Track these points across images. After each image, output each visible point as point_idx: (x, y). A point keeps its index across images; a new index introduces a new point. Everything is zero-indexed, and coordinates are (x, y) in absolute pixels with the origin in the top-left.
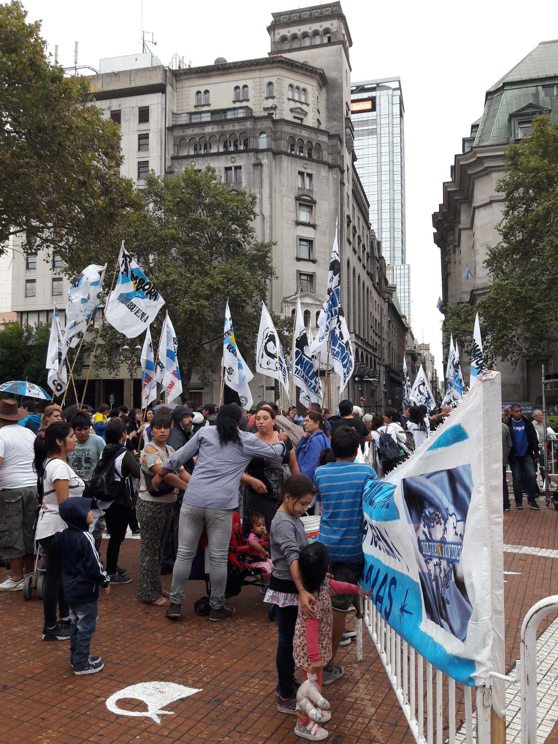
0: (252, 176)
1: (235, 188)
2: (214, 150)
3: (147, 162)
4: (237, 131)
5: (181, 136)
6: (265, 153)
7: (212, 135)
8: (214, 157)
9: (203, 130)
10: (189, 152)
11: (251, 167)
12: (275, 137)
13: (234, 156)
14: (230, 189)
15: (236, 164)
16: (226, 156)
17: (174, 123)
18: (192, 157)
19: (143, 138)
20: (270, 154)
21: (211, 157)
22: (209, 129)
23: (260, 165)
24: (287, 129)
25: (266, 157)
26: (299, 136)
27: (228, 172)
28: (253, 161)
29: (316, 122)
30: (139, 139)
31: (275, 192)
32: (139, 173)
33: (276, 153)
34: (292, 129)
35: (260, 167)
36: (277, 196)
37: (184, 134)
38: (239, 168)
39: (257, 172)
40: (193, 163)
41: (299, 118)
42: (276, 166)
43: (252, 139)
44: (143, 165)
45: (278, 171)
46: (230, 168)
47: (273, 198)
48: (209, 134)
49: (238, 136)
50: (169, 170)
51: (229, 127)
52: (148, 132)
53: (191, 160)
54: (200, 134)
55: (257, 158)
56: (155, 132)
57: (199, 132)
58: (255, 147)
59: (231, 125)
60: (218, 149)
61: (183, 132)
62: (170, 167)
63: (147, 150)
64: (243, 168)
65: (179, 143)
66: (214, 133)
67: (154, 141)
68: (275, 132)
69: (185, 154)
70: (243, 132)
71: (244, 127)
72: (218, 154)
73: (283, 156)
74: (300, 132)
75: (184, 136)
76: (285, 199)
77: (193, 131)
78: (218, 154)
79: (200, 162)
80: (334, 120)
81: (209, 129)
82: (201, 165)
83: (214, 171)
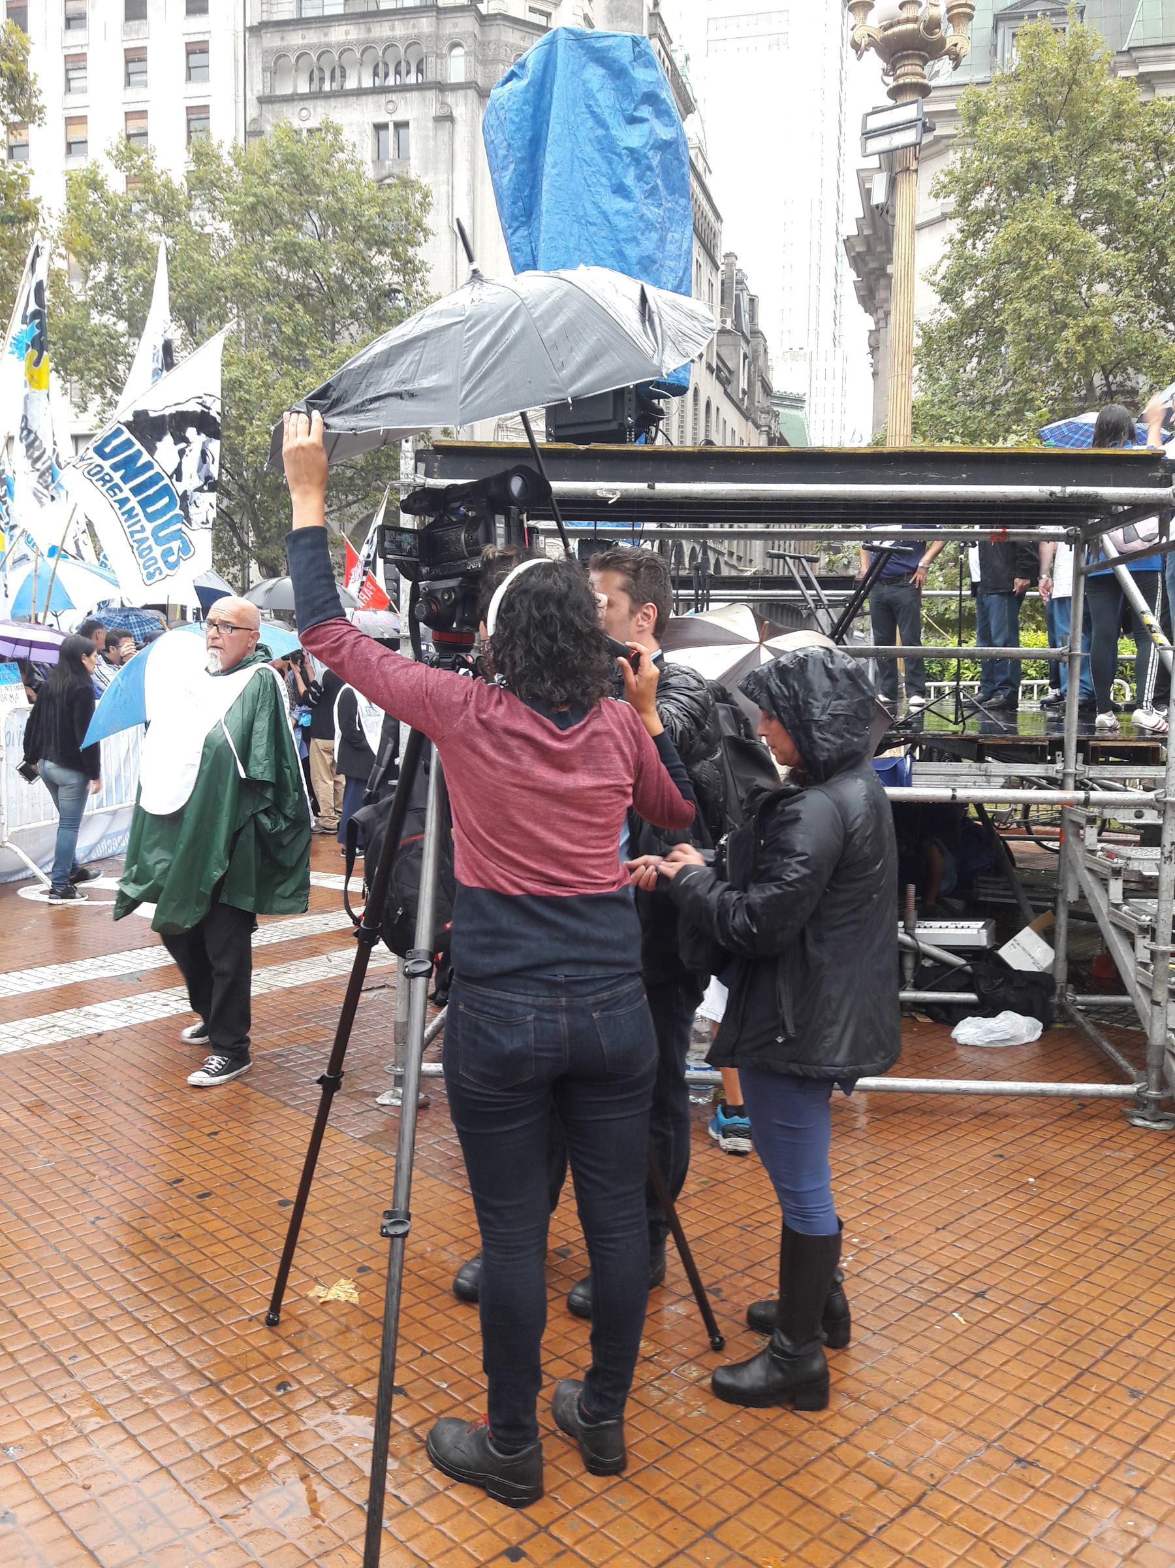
0: (432, 143)
1: (396, 171)
2: (351, 84)
5: (279, 50)
6: (461, 93)
7: (345, 50)
8: (352, 99)
9: (326, 35)
10: (295, 86)
11: (430, 124)
12: (483, 55)
13: (393, 97)
14: (385, 173)
15: (399, 117)
16: (376, 97)
17: (265, 18)
18: (303, 97)
20: (472, 94)
21: (342, 100)
22: (339, 34)
23: (450, 118)
24: (512, 36)
25: (462, 101)
27: (382, 133)
28: (434, 110)
29: (581, 21)
30: (188, 53)
32: (189, 132)
34: (523, 39)
35: (448, 124)
38: (406, 124)
39: (443, 135)
40: (304, 113)
41: (542, 13)
44: (197, 115)
46: (385, 126)
47: (478, 193)
48: (340, 44)
51: (382, 30)
55: (443, 104)
58: (439, 79)
59: (386, 25)
61: (282, 39)
62: (254, 120)
63: (206, 79)
65: (276, 65)
68: (484, 45)
69: (287, 90)
70: (413, 43)
72: (360, 92)
75: (286, 49)
77: (304, 38)
78: (360, 92)
79: (319, 109)
80: (624, 17)
81: (339, 34)
82: (314, 116)
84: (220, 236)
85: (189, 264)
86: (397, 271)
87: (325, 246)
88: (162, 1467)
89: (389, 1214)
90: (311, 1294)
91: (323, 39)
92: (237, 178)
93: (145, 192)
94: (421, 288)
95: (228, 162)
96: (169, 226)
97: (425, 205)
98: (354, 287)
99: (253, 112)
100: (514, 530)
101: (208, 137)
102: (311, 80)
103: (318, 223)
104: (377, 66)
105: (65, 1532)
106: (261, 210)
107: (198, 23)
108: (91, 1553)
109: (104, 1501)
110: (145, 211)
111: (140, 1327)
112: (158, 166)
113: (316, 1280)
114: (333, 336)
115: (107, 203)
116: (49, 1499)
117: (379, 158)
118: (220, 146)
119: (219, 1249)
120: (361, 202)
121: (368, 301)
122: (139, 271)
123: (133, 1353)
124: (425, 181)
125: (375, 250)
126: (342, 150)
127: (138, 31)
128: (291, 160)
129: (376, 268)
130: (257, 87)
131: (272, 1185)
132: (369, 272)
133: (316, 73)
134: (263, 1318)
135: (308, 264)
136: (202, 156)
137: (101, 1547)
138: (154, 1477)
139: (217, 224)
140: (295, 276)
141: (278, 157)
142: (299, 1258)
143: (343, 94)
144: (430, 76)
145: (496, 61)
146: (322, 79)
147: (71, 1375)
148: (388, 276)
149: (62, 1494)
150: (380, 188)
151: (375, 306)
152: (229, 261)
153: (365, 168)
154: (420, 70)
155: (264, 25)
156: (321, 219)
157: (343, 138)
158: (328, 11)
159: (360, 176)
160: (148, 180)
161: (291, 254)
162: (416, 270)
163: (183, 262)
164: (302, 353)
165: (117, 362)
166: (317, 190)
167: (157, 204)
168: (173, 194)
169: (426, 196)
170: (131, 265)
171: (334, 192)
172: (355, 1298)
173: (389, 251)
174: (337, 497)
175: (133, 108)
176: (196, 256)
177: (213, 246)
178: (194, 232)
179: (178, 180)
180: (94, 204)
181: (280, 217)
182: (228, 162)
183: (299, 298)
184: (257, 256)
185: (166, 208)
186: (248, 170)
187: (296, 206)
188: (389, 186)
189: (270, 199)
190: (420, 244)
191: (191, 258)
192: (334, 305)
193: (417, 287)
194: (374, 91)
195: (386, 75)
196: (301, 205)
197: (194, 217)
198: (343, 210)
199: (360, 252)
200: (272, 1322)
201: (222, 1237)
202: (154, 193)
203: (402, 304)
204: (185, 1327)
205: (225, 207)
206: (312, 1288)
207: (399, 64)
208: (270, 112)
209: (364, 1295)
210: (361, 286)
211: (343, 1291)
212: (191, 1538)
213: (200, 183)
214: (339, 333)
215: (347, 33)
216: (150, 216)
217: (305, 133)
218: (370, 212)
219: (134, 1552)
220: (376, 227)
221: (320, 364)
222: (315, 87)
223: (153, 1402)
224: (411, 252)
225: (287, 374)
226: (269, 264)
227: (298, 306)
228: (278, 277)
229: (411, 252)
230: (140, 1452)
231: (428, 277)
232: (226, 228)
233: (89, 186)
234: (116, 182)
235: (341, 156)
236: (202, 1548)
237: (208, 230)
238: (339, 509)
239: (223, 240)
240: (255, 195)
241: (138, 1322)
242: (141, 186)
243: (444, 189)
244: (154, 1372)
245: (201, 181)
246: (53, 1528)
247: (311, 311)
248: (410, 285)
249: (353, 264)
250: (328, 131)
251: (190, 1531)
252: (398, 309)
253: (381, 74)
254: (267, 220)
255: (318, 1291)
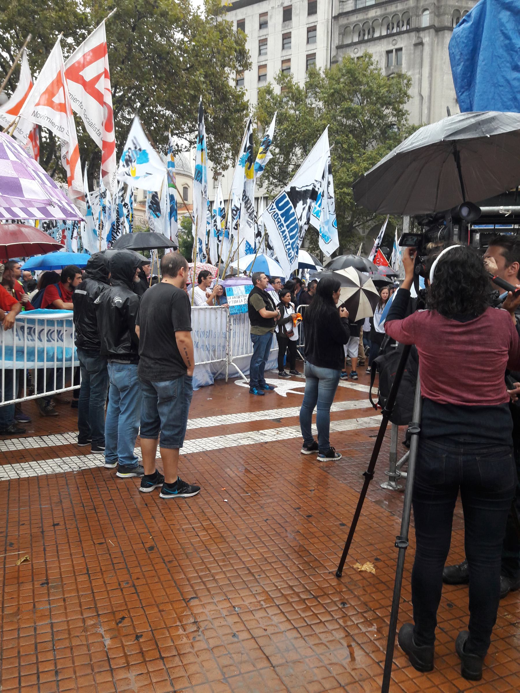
0: (412, 56)
1: (396, 71)
2: (377, 35)
3: (314, 54)
4: (401, 11)
5: (346, 24)
6: (427, 31)
7: (375, 20)
8: (377, 41)
9: (367, 14)
10: (352, 39)
11: (412, 48)
13: (396, 38)
14: (390, 72)
15: (397, 46)
19: (312, 30)
20: (432, 31)
21: (372, 43)
22: (372, 13)
23: (421, 44)
25: (427, 35)
26: (465, 7)
27: (390, 55)
28: (414, 40)
30: (308, 32)
31: (436, 71)
32: (307, 65)
33: (438, 30)
35: (420, 46)
36: (437, 75)
37: (349, 21)
38: (400, 49)
39: (418, 52)
40: (356, 50)
42: (438, 43)
43: (414, 18)
44: (311, 58)
45: (440, 48)
48: (372, 18)
49: (401, 16)
50: (334, 59)
52: (316, 24)
53: (355, 47)
54: (364, 20)
55: (419, 37)
56: (322, 23)
57: (362, 18)
60: (381, 33)
61: (348, 19)
62: (334, 57)
63: (315, 42)
64: (403, 49)
65: (344, 31)
66: (377, 16)
67: (321, 33)
69: (349, 42)
71: (407, 6)
72: (381, 38)
73: (446, 31)
74: (467, 3)
75: (349, 24)
76: (445, 78)
78: (381, 38)
79: (363, 48)
81: (372, 13)
82: (360, 51)
83: (370, 57)
84: (318, 108)
85: (305, 121)
86: (394, 116)
87: (363, 108)
88: (295, 628)
89: (399, 538)
90: (355, 566)
91: (365, 17)
92: (326, 82)
93: (288, 93)
94: (405, 122)
95: (323, 75)
96: (298, 106)
97: (408, 85)
98: (375, 125)
99: (334, 53)
100: (463, 233)
101: (315, 66)
102: (359, 35)
103: (360, 98)
104: (388, 25)
105: (257, 646)
106: (336, 95)
107: (312, 18)
108: (267, 657)
109: (272, 637)
110: (288, 101)
111: (284, 568)
112: (294, 81)
113: (357, 560)
114: (365, 147)
115: (273, 99)
116: (251, 631)
117: (388, 66)
118: (320, 69)
119: (316, 540)
120: (379, 86)
121: (381, 130)
122: (285, 126)
123: (282, 578)
124: (409, 74)
125: (385, 107)
126: (372, 64)
127: (288, 26)
128: (350, 72)
129: (385, 115)
130: (336, 42)
131: (337, 516)
132: (382, 117)
133: (362, 32)
134: (335, 573)
135: (355, 116)
136: (312, 74)
137: (271, 656)
138: (292, 631)
139: (317, 103)
140: (349, 122)
141: (344, 71)
142: (350, 551)
143: (373, 39)
144: (413, 26)
145: (444, 14)
146: (364, 35)
147: (258, 583)
148: (390, 119)
149: (256, 630)
150: (388, 79)
151: (384, 132)
152: (322, 118)
153: (382, 71)
154: (408, 24)
155: (341, 15)
156: (361, 96)
157: (373, 59)
158: (368, 4)
159: (379, 75)
160: (290, 88)
161: (349, 113)
162: (403, 115)
163: (303, 121)
164: (351, 156)
165: (275, 166)
166: (360, 83)
167: (293, 98)
168: (299, 92)
169: (409, 80)
170: (282, 124)
171: (367, 83)
172: (374, 571)
173: (391, 107)
174: (362, 218)
175: (285, 58)
176: (308, 117)
177: (315, 113)
178: (307, 108)
179: (302, 86)
180: (269, 100)
181: (344, 97)
182: (323, 75)
183: (351, 132)
184: (334, 115)
185: (297, 99)
186: (331, 78)
187: (351, 91)
188: (393, 78)
189: (340, 90)
190: (405, 103)
191: (306, 119)
192: (366, 133)
193: (403, 122)
194: (387, 36)
195: (393, 28)
196: (353, 90)
197: (308, 101)
198: (371, 91)
199: (378, 109)
200: (338, 575)
201: (317, 535)
202: (292, 93)
203: (396, 130)
204: (303, 571)
205: (321, 95)
206: (355, 564)
207: (398, 23)
208: (341, 52)
209: (378, 570)
210: (378, 124)
211: (368, 567)
212: (307, 660)
213: (310, 86)
214: (367, 146)
215: (376, 12)
216: (290, 103)
217: (356, 59)
218: (384, 90)
219: (284, 661)
220: (386, 97)
221: (358, 160)
222: (361, 38)
223: (291, 600)
224: (401, 107)
225: (344, 166)
226: (339, 118)
227: (350, 135)
228: (342, 123)
229: (401, 107)
230: (285, 619)
231: (408, 117)
232: (321, 104)
233: (267, 93)
234: (277, 90)
235: (372, 67)
236: (312, 666)
237: (313, 106)
238: (363, 223)
239: (319, 109)
240: (334, 89)
241: (284, 565)
242: (287, 90)
243: (417, 76)
244: (291, 587)
245: (311, 85)
246: (252, 644)
247: (355, 137)
248: (400, 122)
249: (375, 114)
250: (366, 57)
251: (306, 657)
252: (394, 133)
253: (391, 28)
254: (338, 99)
255: (357, 565)
